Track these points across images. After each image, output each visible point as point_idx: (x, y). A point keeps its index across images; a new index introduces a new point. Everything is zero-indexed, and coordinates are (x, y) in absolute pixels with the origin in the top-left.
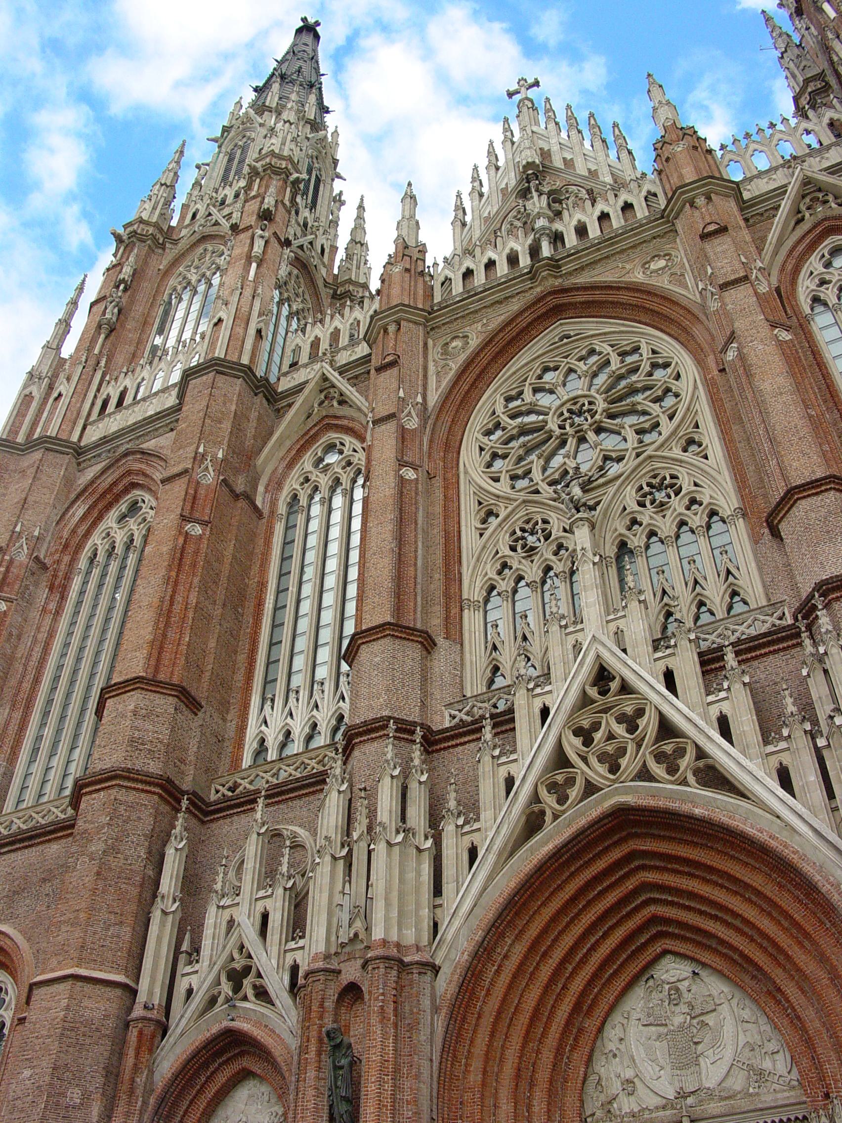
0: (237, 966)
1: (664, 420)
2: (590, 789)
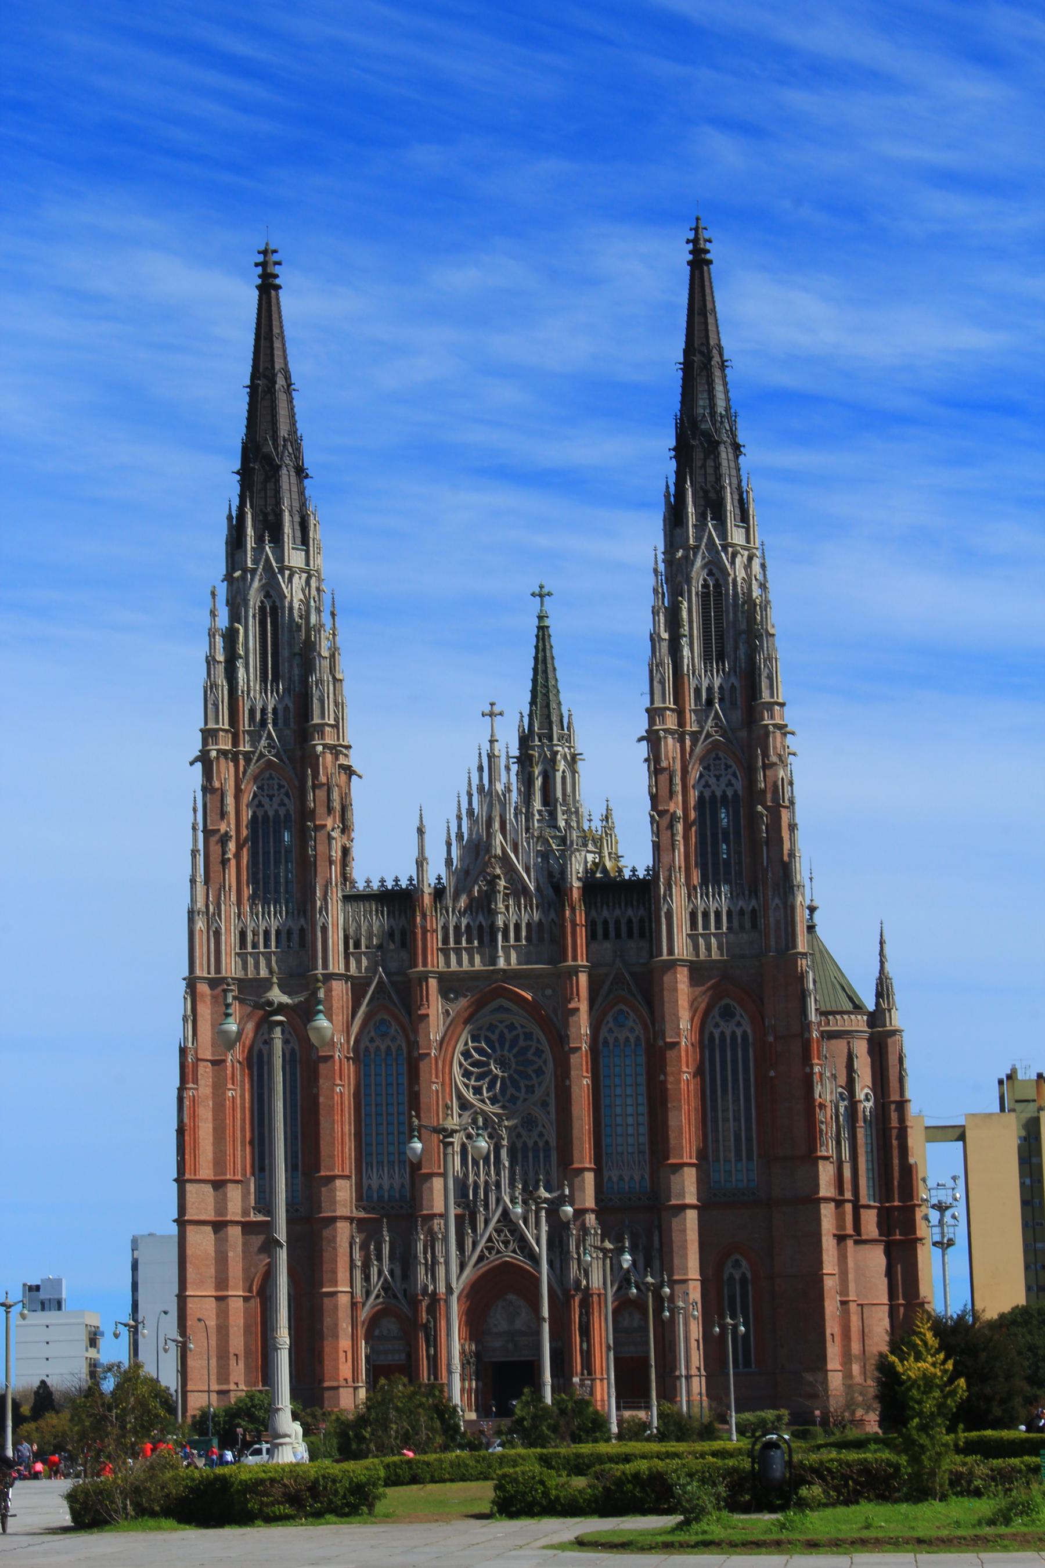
0: (386, 1286)
1: (537, 1085)
2: (499, 1252)
